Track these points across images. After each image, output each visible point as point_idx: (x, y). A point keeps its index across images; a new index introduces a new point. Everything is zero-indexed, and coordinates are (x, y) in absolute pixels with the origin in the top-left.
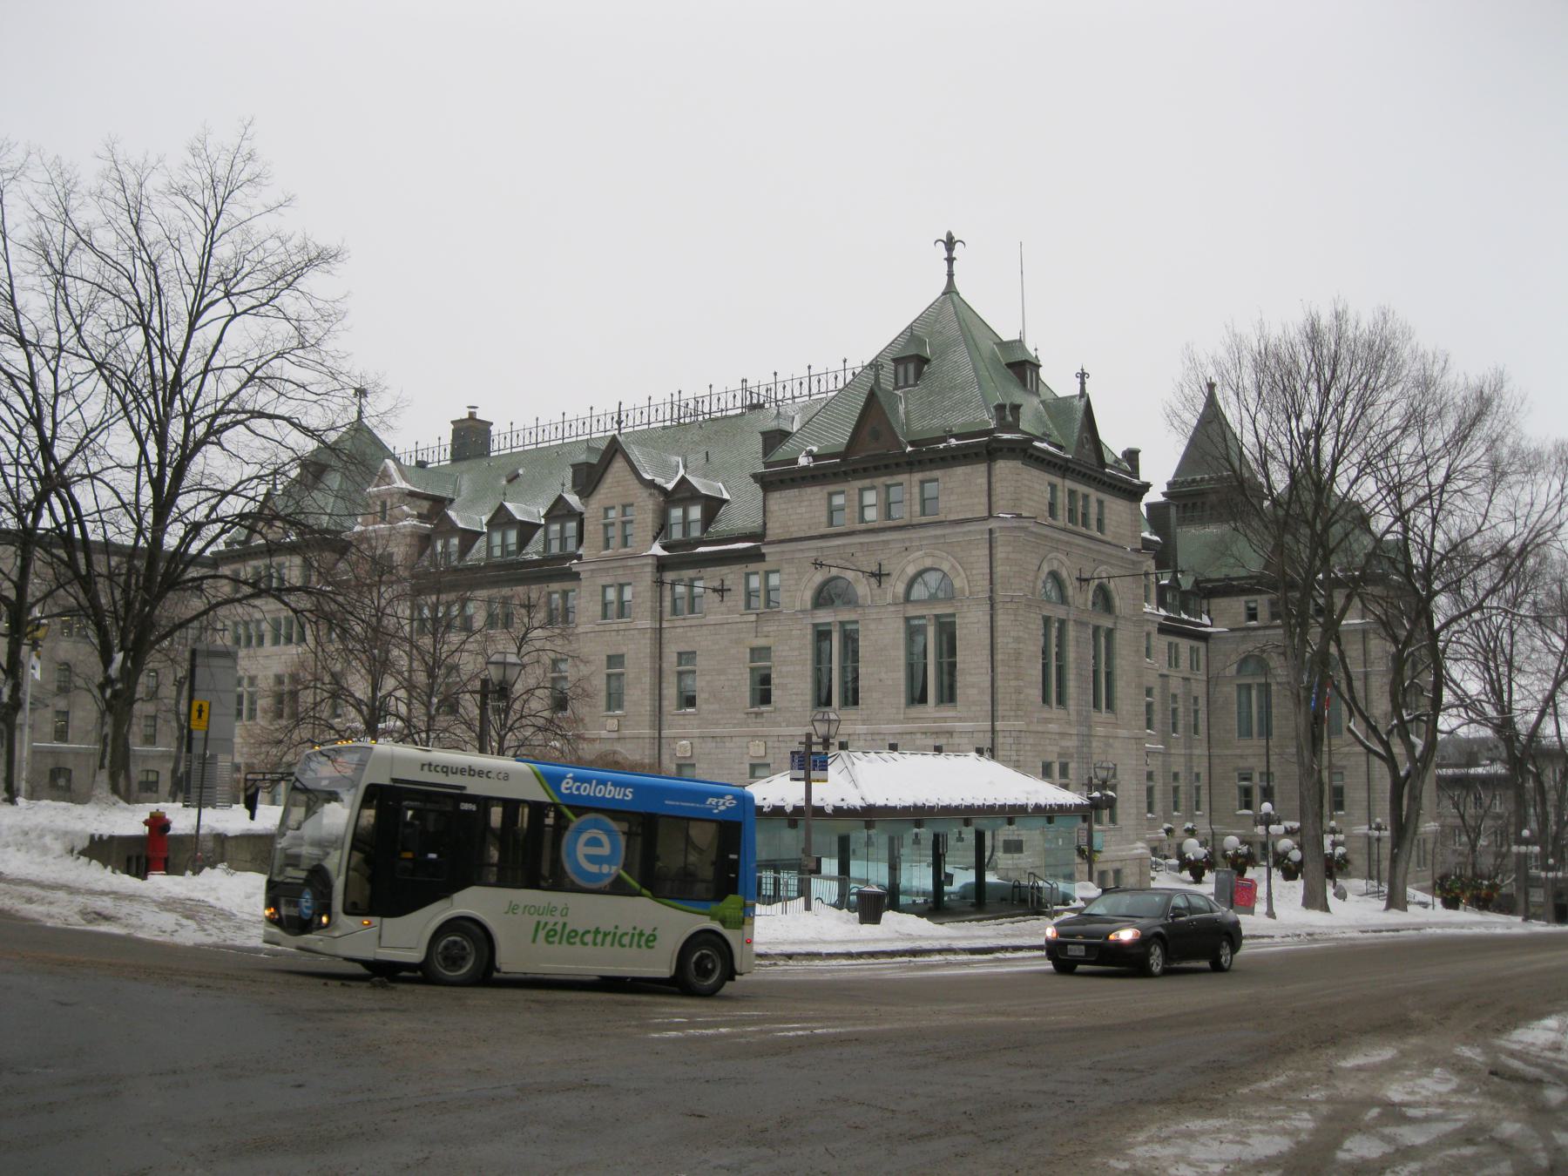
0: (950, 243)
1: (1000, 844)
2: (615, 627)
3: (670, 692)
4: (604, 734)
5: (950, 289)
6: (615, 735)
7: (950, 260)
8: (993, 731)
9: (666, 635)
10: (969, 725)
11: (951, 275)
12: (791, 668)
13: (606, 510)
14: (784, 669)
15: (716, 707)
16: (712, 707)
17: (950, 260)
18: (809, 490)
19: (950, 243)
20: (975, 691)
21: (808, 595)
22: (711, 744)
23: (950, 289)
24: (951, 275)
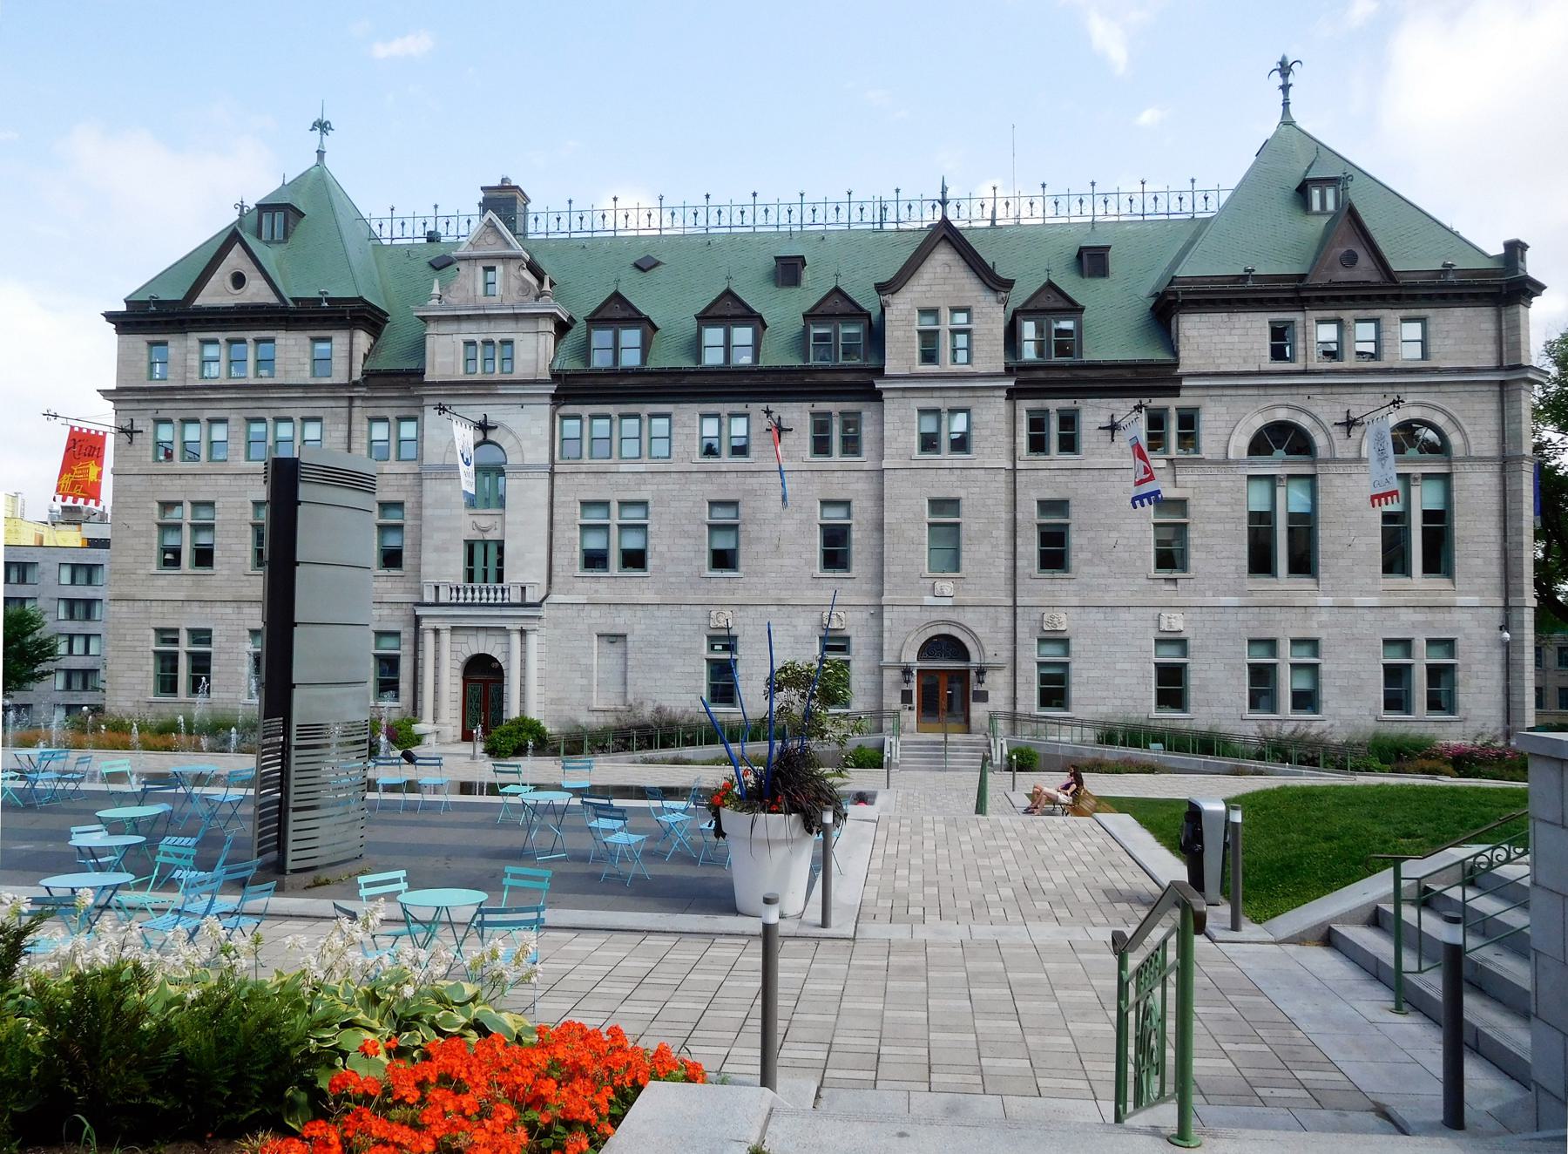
0: (1285, 69)
1: (1170, 716)
2: (947, 464)
3: (1030, 548)
4: (929, 600)
5: (1287, 121)
6: (949, 602)
7: (1285, 88)
8: (1507, 607)
9: (1020, 477)
10: (1474, 600)
11: (1286, 104)
12: (1219, 527)
13: (967, 310)
14: (1209, 527)
15: (1105, 570)
16: (1097, 570)
17: (1285, 88)
18: (1243, 317)
19: (1285, 69)
20: (1479, 561)
21: (1240, 443)
22: (1095, 616)
23: (1287, 121)
24: (1286, 104)
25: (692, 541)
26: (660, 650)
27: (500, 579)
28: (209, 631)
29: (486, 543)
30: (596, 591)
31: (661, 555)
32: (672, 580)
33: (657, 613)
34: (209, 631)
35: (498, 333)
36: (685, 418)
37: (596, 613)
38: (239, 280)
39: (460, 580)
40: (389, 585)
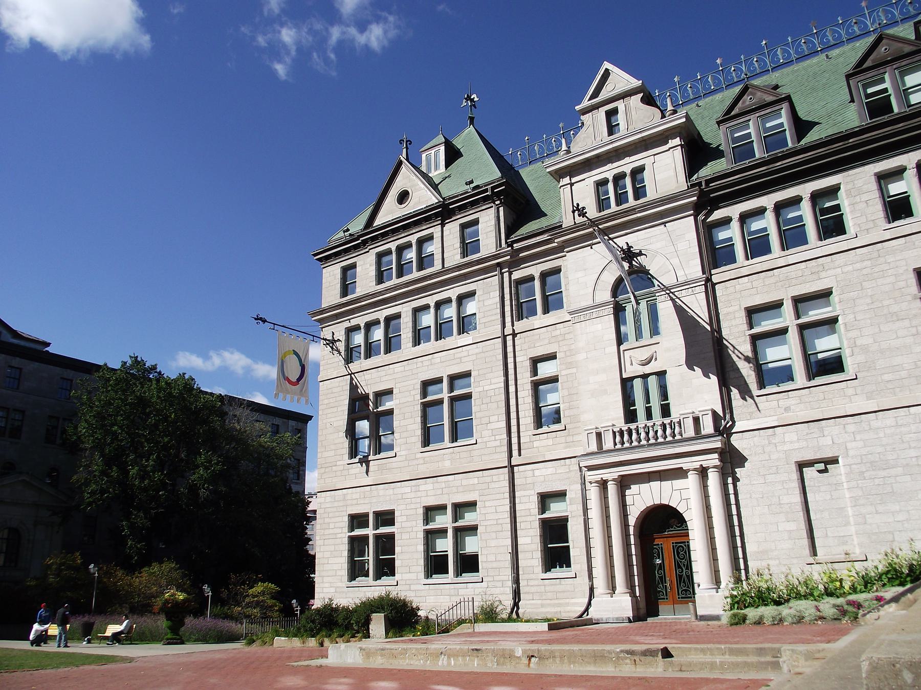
25: (906, 323)
26: (893, 472)
27: (666, 411)
28: (392, 513)
29: (645, 377)
30: (787, 409)
31: (865, 349)
32: (886, 377)
33: (875, 424)
34: (392, 513)
35: (627, 165)
36: (859, 183)
37: (790, 434)
38: (403, 197)
39: (621, 424)
40: (550, 442)
